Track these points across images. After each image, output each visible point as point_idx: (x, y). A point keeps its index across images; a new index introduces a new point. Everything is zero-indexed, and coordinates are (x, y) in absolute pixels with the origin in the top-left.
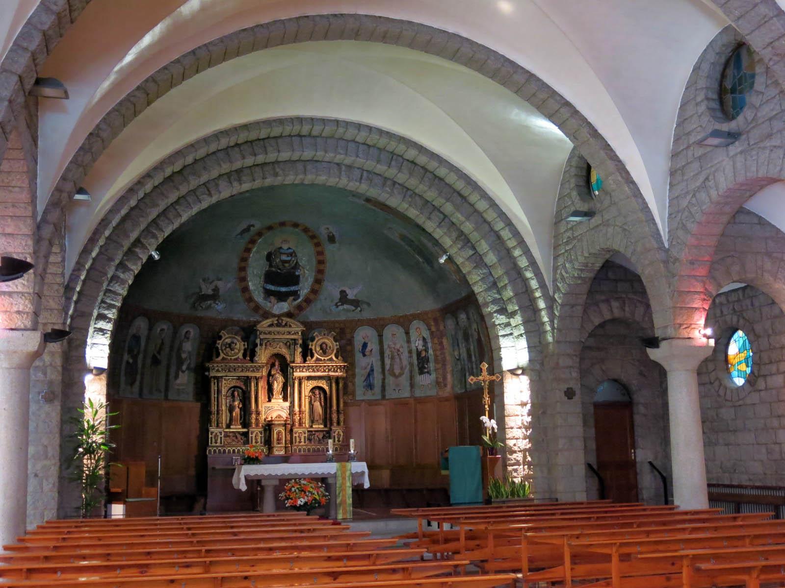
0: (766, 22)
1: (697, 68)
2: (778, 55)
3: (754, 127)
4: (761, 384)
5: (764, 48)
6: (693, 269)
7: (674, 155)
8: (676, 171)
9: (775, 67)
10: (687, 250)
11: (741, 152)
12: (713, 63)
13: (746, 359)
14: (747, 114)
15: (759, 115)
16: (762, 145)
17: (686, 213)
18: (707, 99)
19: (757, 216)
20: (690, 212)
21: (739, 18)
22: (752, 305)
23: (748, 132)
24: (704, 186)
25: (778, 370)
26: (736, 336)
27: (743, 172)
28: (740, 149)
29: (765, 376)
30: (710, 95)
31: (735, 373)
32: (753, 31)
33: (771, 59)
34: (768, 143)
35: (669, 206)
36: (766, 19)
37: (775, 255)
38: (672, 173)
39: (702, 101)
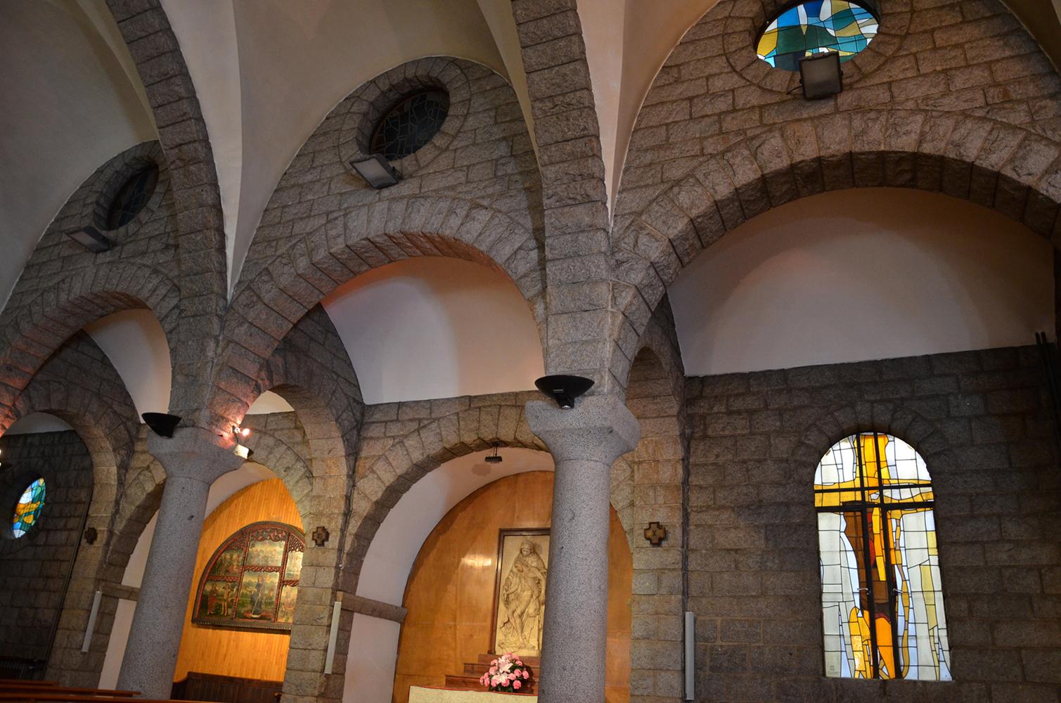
0: (183, 121)
1: (100, 171)
2: (181, 160)
3: (131, 242)
4: (41, 539)
5: (171, 148)
6: (8, 376)
7: (39, 249)
8: (33, 266)
9: (175, 172)
10: (9, 352)
11: (109, 262)
12: (117, 172)
13: (36, 511)
14: (132, 227)
15: (141, 231)
16: (132, 260)
17: (25, 311)
18: (97, 203)
19: (102, 352)
20: (30, 311)
21: (159, 106)
22: (65, 452)
23: (124, 245)
24: (56, 288)
25: (65, 525)
26: (35, 484)
27: (104, 281)
28: (108, 260)
29: (48, 531)
30: (102, 201)
31: (18, 525)
32: (168, 126)
33: (173, 162)
34: (138, 261)
35: (9, 300)
36: (185, 118)
37: (105, 399)
38: (28, 267)
39: (92, 203)
